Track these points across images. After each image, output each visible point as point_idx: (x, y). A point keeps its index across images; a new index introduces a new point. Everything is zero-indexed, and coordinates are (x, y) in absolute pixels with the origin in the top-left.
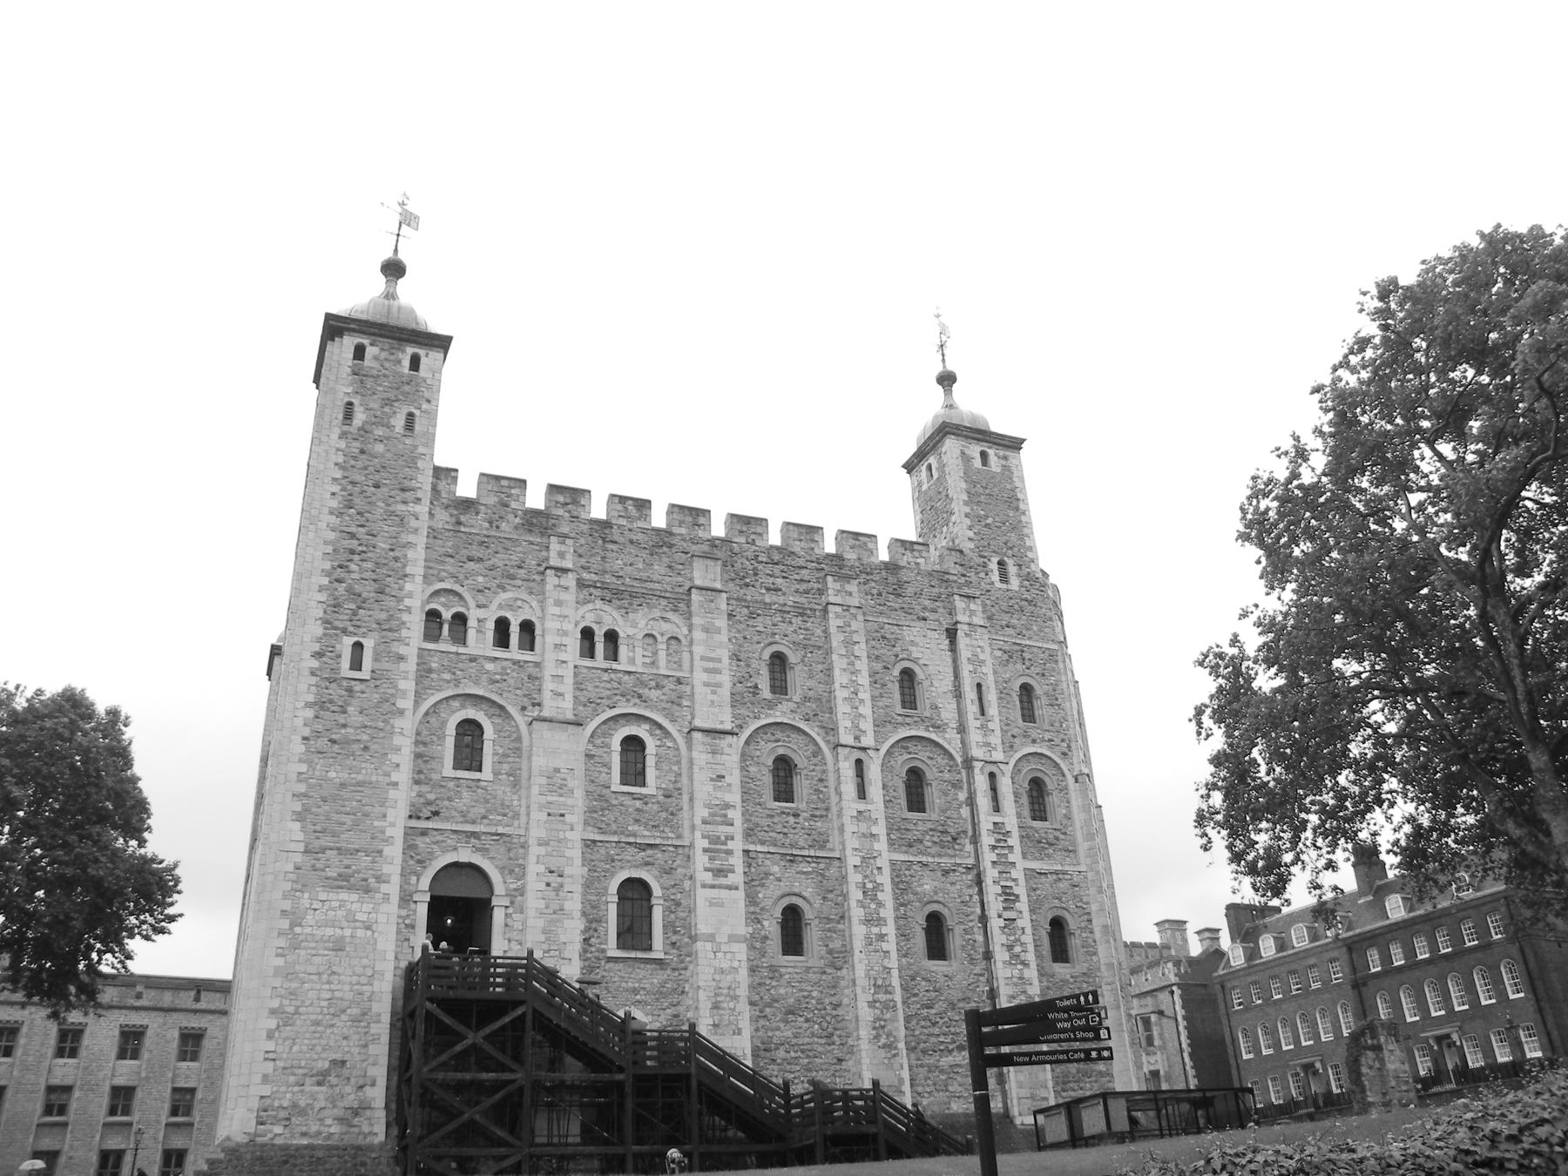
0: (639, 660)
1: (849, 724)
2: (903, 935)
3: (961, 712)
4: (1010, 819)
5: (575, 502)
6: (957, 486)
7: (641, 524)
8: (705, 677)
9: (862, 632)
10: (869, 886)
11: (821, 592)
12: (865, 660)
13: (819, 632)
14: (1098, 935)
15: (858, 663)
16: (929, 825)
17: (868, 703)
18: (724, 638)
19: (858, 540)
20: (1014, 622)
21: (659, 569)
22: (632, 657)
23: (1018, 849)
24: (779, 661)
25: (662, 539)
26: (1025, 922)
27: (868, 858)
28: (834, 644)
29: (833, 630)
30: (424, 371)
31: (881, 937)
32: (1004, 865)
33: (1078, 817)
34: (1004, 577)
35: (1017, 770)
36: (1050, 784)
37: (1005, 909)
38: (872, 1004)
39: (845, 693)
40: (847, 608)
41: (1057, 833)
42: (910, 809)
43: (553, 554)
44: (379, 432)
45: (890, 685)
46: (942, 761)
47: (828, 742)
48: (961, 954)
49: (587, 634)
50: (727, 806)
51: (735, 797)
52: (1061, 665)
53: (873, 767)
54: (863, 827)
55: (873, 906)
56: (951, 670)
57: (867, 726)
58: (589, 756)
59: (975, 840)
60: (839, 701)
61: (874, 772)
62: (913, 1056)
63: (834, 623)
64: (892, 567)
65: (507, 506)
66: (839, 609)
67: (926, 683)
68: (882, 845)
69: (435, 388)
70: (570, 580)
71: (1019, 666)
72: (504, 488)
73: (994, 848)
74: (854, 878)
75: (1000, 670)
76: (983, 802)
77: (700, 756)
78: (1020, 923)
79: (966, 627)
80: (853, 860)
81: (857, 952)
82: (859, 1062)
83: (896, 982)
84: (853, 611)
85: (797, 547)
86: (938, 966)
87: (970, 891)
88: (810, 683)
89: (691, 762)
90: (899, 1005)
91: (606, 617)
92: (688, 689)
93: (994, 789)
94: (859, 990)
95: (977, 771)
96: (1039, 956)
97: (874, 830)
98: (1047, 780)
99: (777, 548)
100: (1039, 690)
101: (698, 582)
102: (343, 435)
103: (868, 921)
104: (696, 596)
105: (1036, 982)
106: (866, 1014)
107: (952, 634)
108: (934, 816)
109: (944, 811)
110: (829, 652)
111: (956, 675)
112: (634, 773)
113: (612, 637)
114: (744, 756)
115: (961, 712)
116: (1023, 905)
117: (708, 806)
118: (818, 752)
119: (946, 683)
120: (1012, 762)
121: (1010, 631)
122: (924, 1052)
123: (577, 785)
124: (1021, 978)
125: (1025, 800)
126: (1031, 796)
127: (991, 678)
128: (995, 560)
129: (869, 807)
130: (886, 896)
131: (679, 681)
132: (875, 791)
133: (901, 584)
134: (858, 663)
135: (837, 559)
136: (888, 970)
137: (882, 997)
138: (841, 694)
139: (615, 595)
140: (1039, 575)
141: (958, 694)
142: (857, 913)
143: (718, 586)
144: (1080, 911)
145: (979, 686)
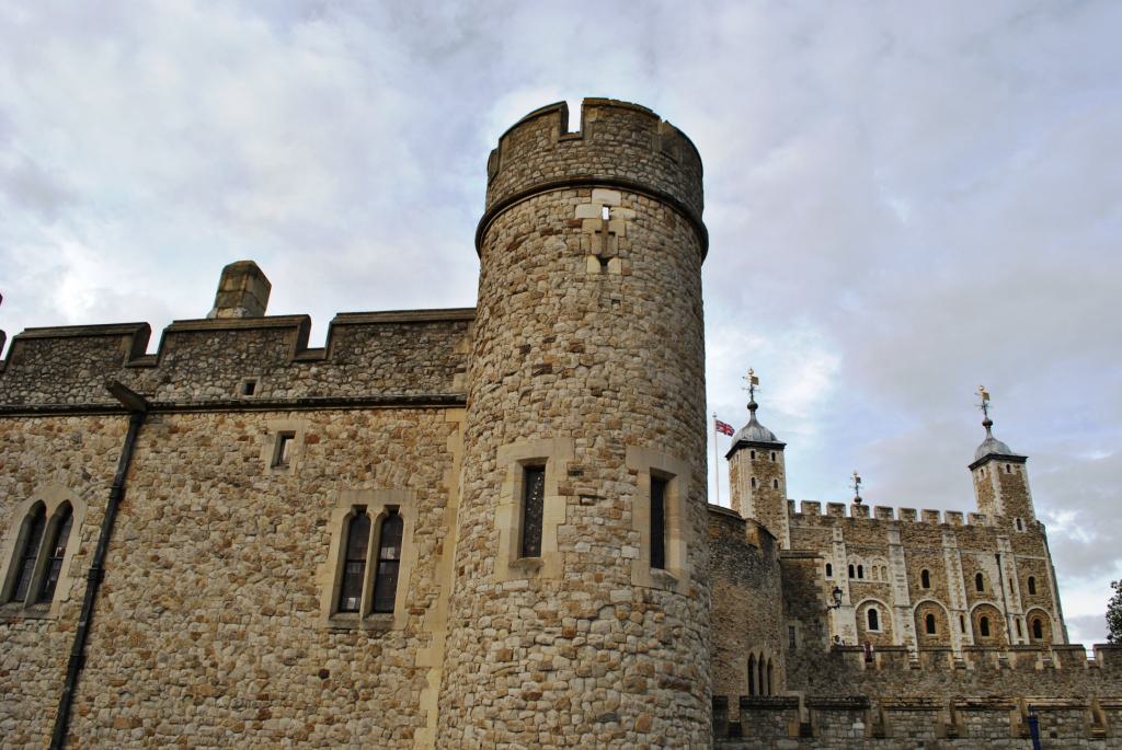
0: (872, 577)
5: (840, 511)
8: (898, 583)
11: (941, 541)
18: (904, 566)
19: (955, 515)
21: (875, 537)
22: (868, 576)
24: (925, 575)
25: (875, 524)
30: (777, 461)
34: (1020, 528)
35: (1027, 618)
36: (1044, 622)
39: (954, 587)
43: (834, 535)
44: (766, 490)
46: (995, 614)
49: (851, 568)
50: (911, 638)
51: (914, 634)
57: (964, 600)
58: (857, 618)
61: (968, 621)
64: (970, 527)
69: (783, 468)
70: (843, 546)
72: (813, 506)
77: (900, 618)
85: (929, 522)
89: (896, 621)
91: (858, 560)
92: (891, 589)
99: (921, 523)
100: (1037, 579)
101: (891, 542)
102: (753, 493)
104: (891, 549)
107: (998, 557)
111: (1001, 574)
112: (874, 625)
113: (860, 568)
114: (916, 615)
117: (904, 637)
118: (944, 613)
119: (995, 580)
126: (1034, 627)
131: (888, 585)
135: (946, 526)
138: (952, 587)
139: (863, 551)
141: (1001, 584)
143: (899, 542)
145: (1011, 580)
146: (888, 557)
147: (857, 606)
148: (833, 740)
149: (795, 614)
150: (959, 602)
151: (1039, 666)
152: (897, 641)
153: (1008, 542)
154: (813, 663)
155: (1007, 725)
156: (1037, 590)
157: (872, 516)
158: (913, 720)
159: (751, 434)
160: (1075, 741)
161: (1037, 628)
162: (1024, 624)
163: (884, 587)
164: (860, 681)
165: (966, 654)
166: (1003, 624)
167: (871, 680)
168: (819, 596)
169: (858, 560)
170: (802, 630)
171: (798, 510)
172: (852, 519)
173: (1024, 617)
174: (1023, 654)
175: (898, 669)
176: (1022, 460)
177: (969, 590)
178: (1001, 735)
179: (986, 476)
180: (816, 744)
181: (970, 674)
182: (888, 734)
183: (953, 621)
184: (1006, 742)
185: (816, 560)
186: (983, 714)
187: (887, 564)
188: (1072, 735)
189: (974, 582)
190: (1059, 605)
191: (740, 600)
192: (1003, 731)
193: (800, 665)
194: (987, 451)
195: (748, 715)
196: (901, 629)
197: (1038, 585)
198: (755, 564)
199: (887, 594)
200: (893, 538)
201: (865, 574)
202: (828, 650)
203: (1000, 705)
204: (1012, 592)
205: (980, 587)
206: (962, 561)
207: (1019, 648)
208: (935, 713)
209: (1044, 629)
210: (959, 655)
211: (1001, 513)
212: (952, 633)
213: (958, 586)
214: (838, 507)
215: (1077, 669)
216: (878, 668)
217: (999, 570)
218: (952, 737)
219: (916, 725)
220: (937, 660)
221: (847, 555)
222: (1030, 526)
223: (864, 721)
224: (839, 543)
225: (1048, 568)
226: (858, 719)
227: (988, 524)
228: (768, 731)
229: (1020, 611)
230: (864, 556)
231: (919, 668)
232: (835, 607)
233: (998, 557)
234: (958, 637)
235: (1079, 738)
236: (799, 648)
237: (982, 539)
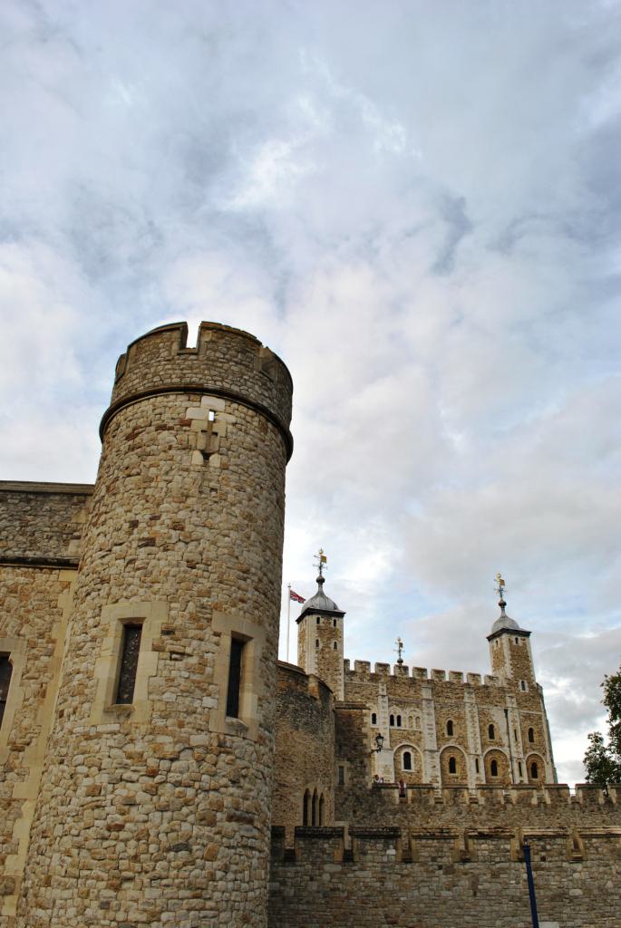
6: (507, 653)
7: (405, 676)
8: (428, 731)
11: (463, 698)
19: (474, 676)
21: (412, 692)
24: (450, 725)
25: (413, 681)
30: (338, 626)
34: (524, 689)
36: (539, 765)
43: (380, 690)
49: (392, 717)
51: (439, 774)
56: (505, 727)
57: (479, 746)
61: (481, 763)
64: (486, 687)
65: (364, 672)
69: (342, 632)
70: (386, 699)
71: (529, 722)
77: (429, 760)
85: (455, 681)
89: (425, 762)
91: (397, 711)
101: (425, 697)
102: (317, 652)
104: (424, 702)
107: (506, 711)
112: (408, 766)
113: (399, 717)
114: (441, 758)
118: (463, 756)
119: (503, 730)
123: (392, 770)
125: (530, 771)
126: (532, 769)
127: (519, 727)
128: (520, 681)
132: (482, 770)
135: (468, 685)
138: (470, 735)
139: (401, 704)
141: (508, 734)
143: (431, 698)
146: (422, 710)
147: (395, 750)
148: (370, 864)
149: (345, 755)
151: (534, 801)
152: (426, 780)
153: (514, 700)
154: (358, 798)
155: (508, 851)
156: (535, 739)
157: (411, 675)
158: (435, 847)
159: (318, 604)
160: (559, 864)
161: (534, 770)
162: (524, 767)
163: (417, 734)
164: (394, 813)
165: (479, 791)
166: (508, 766)
167: (403, 812)
168: (365, 741)
169: (397, 711)
170: (349, 769)
171: (352, 668)
172: (395, 677)
173: (524, 761)
174: (522, 791)
175: (425, 803)
176: (527, 634)
177: (484, 737)
178: (503, 859)
179: (499, 646)
180: (356, 868)
181: (481, 808)
182: (414, 860)
183: (470, 763)
184: (507, 865)
185: (364, 711)
186: (489, 842)
187: (420, 715)
188: (557, 859)
189: (487, 732)
190: (551, 751)
191: (300, 743)
192: (504, 856)
193: (346, 799)
194: (501, 626)
195: (301, 842)
196: (429, 770)
197: (536, 735)
198: (315, 712)
199: (419, 740)
200: (426, 694)
201: (403, 723)
202: (370, 786)
203: (503, 834)
205: (492, 736)
206: (479, 714)
207: (519, 787)
208: (452, 841)
209: (539, 771)
210: (474, 792)
211: (510, 676)
212: (468, 773)
214: (384, 667)
215: (563, 804)
216: (410, 802)
217: (507, 722)
218: (465, 861)
219: (438, 851)
220: (456, 796)
221: (389, 706)
222: (532, 687)
223: (395, 848)
224: (383, 696)
225: (543, 721)
226: (391, 846)
227: (500, 685)
228: (318, 857)
229: (521, 756)
230: (403, 708)
231: (442, 803)
232: (377, 751)
233: (506, 711)
234: (474, 777)
235: (563, 861)
236: (346, 785)
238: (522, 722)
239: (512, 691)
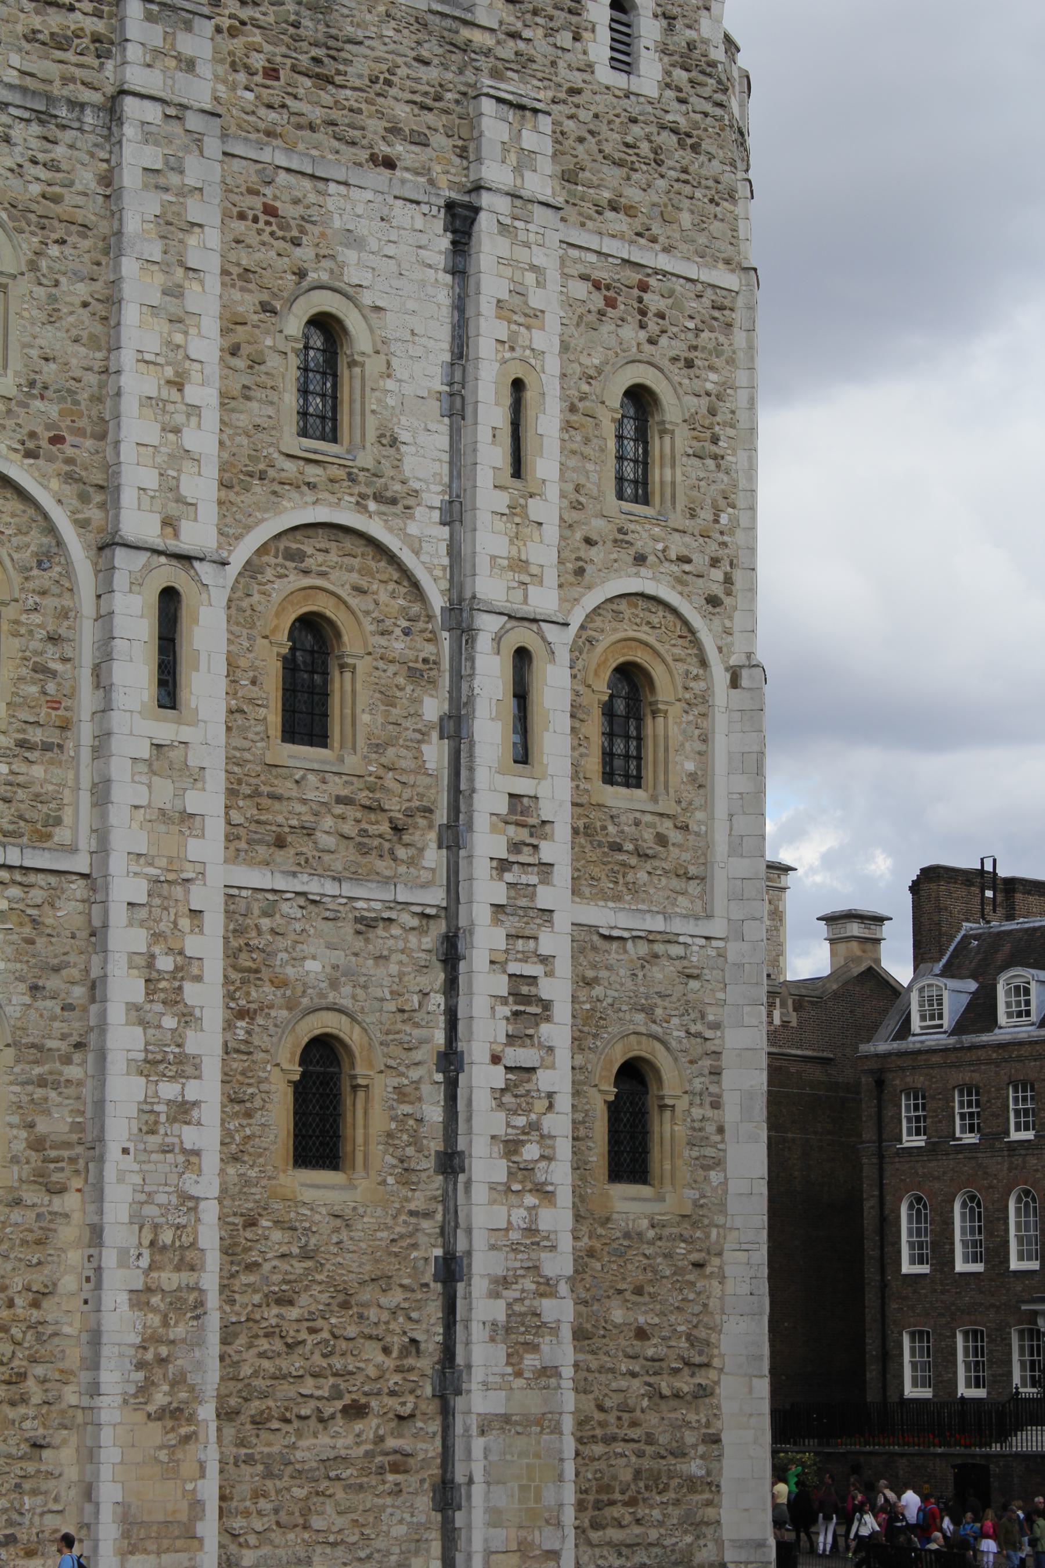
1: (150, 479)
2: (238, 1101)
3: (459, 459)
4: (554, 789)
9: (214, 194)
10: (165, 963)
11: (105, 47)
12: (213, 282)
13: (87, 178)
14: (731, 1113)
15: (193, 288)
16: (337, 787)
17: (211, 418)
20: (632, 194)
23: (563, 874)
26: (556, 1079)
27: (169, 884)
28: (132, 225)
29: (130, 178)
31: (183, 1111)
32: (522, 915)
33: (724, 784)
35: (584, 642)
37: (512, 1039)
38: (140, 1299)
40: (177, 112)
41: (666, 827)
42: (291, 733)
45: (273, 362)
47: (82, 524)
48: (382, 1158)
52: (739, 338)
53: (204, 613)
54: (164, 791)
55: (170, 1022)
57: (202, 487)
59: (454, 838)
60: (129, 406)
61: (207, 632)
62: (229, 1432)
63: (137, 155)
66: (153, 112)
67: (373, 366)
68: (208, 848)
71: (630, 333)
73: (503, 865)
74: (126, 939)
75: (579, 339)
76: (490, 732)
78: (545, 1080)
79: (503, 205)
80: (126, 887)
81: (113, 1152)
82: (90, 1455)
83: (209, 1236)
84: (194, 122)
86: (318, 1188)
87: (423, 981)
88: (51, 338)
90: (213, 1300)
93: (521, 695)
94: (109, 1259)
95: (484, 643)
96: (579, 1166)
97: (193, 802)
98: (658, 672)
100: (673, 407)
103: (153, 1065)
105: (566, 1243)
106: (121, 1323)
107: (461, 220)
108: (352, 762)
109: (378, 748)
110: (112, 245)
115: (459, 459)
116: (558, 1032)
119: (423, 371)
120: (577, 619)
121: (617, 222)
122: (259, 1422)
124: (531, 1231)
125: (594, 727)
126: (608, 711)
127: (553, 365)
129: (186, 733)
130: (207, 996)
132: (205, 685)
133: (335, 46)
134: (193, 288)
136: (189, 1202)
137: (169, 1279)
138: (136, 384)
140: (718, 54)
141: (457, 406)
142: (124, 1040)
144: (696, 1047)
145: (518, 385)
150: (171, 489)
189: (286, 372)
204: (518, 469)
213: (179, 385)
233: (461, 220)
237: (381, 82)
238: (590, 321)
239: (523, 63)
